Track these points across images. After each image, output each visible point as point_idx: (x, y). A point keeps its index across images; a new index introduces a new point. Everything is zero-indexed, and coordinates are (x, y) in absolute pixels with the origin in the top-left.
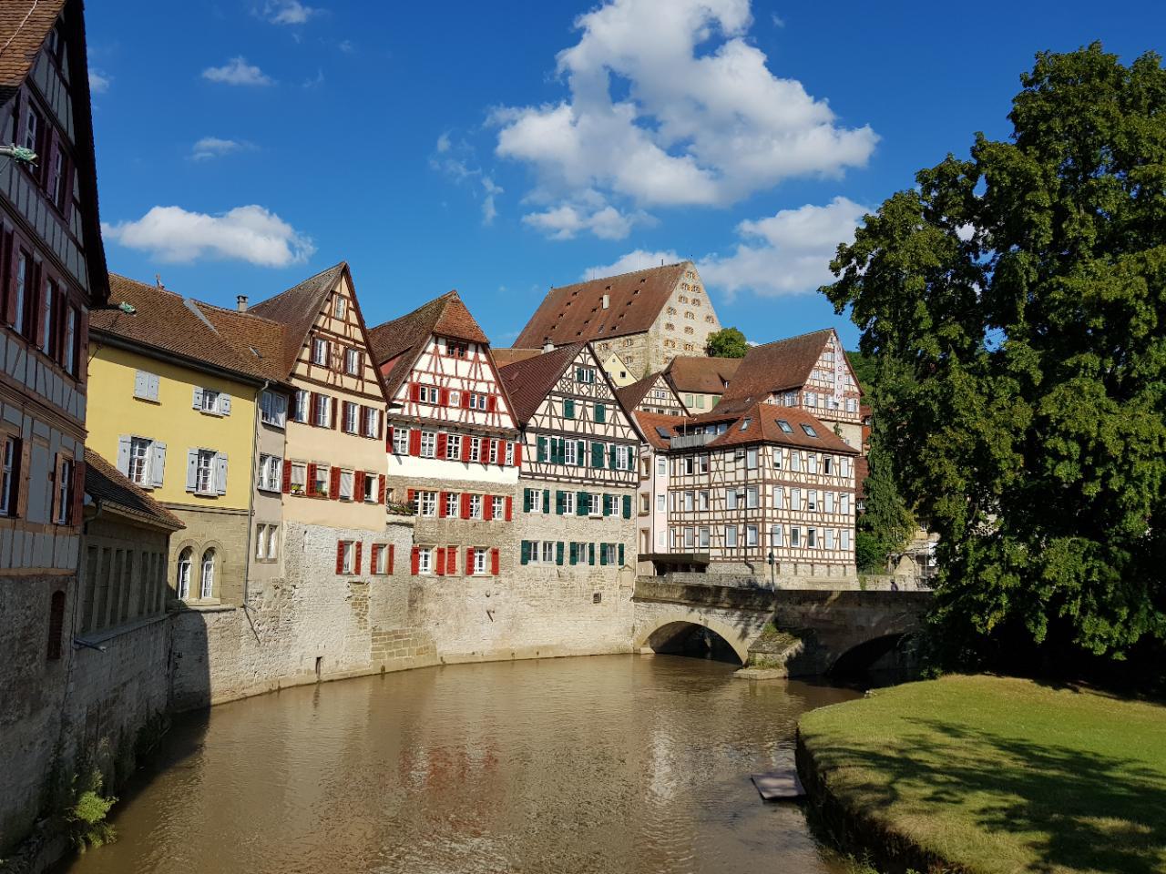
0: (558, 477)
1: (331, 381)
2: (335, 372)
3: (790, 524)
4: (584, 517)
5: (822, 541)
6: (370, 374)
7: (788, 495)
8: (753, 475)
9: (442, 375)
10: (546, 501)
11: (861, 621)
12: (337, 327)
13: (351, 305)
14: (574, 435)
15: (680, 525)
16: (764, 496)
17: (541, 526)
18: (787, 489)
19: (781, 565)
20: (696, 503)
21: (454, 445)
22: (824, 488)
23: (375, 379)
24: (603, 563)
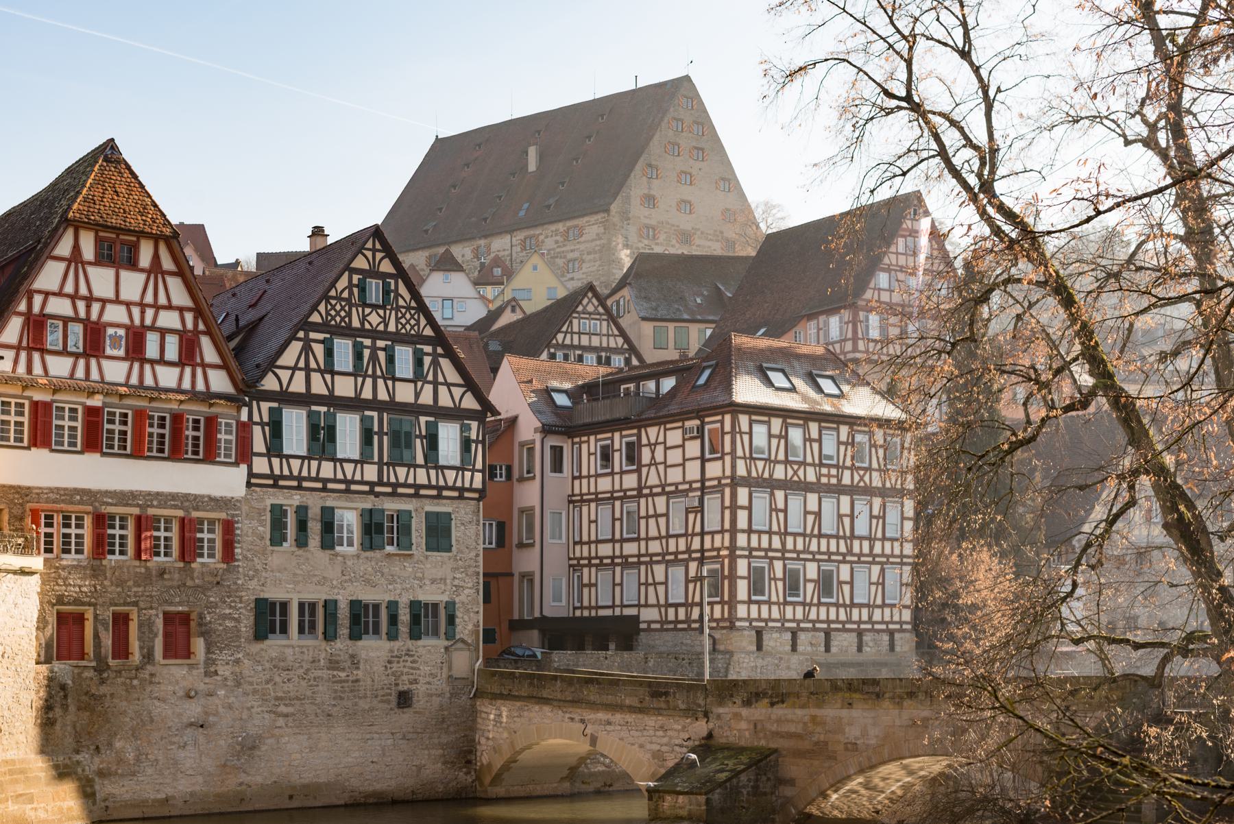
3: (783, 558)
4: (377, 554)
5: (846, 588)
7: (781, 505)
8: (714, 469)
9: (89, 300)
10: (302, 526)
11: (852, 733)
14: (354, 404)
15: (590, 565)
16: (734, 507)
18: (780, 495)
19: (765, 637)
21: (117, 427)
22: (852, 491)
24: (415, 635)
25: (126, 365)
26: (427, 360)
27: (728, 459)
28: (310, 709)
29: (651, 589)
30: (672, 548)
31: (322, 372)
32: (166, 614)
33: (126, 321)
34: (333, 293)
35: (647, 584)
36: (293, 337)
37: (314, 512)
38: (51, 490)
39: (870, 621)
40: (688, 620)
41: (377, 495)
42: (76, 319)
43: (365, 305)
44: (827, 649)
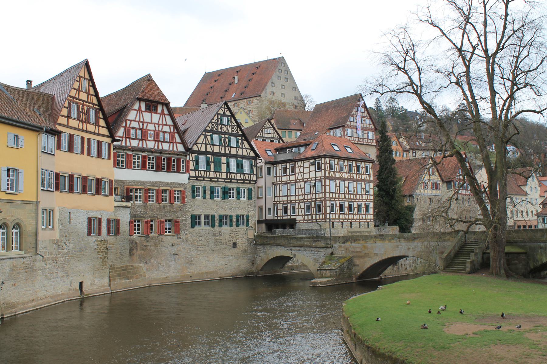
0: (211, 178)
1: (80, 127)
2: (83, 122)
3: (339, 201)
4: (226, 201)
6: (102, 123)
7: (338, 185)
9: (143, 122)
10: (205, 192)
13: (91, 84)
15: (280, 203)
16: (325, 186)
18: (338, 181)
21: (151, 162)
22: (356, 180)
23: (105, 125)
24: (237, 225)
25: (154, 142)
26: (240, 141)
27: (323, 171)
29: (300, 210)
30: (306, 198)
31: (210, 145)
33: (154, 129)
34: (213, 121)
35: (298, 209)
36: (202, 134)
37: (208, 188)
38: (132, 181)
39: (362, 219)
40: (312, 219)
41: (226, 182)
42: (139, 129)
44: (351, 227)
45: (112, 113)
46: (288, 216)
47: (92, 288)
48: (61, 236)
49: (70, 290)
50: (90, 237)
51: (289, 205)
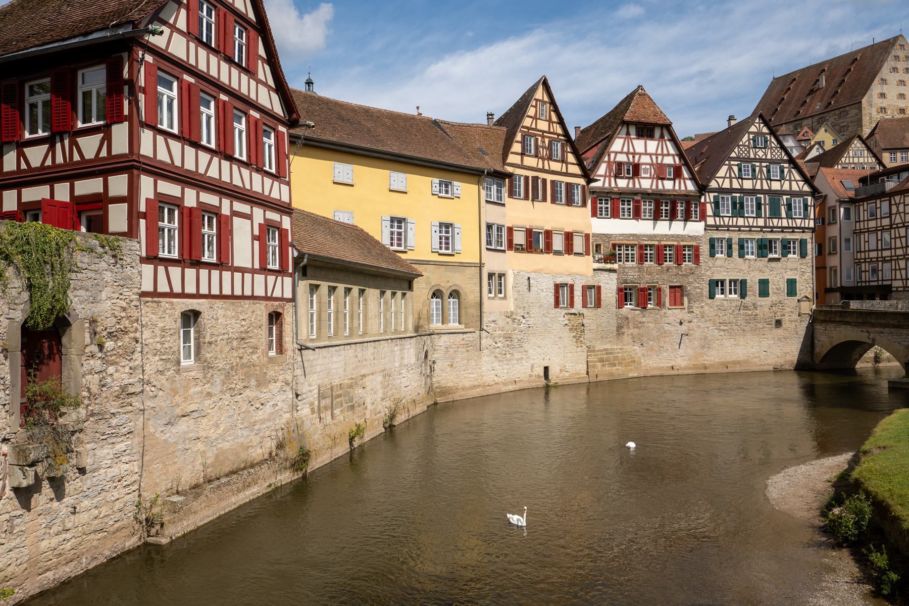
1: (540, 166)
2: (543, 159)
6: (571, 158)
9: (634, 154)
10: (730, 247)
12: (543, 125)
14: (753, 192)
17: (723, 267)
20: (879, 242)
23: (575, 162)
25: (650, 181)
26: (786, 170)
28: (735, 327)
29: (898, 272)
31: (737, 179)
32: (671, 287)
35: (896, 270)
37: (735, 241)
38: (621, 235)
41: (764, 232)
43: (755, 148)
45: (588, 145)
46: (878, 281)
47: (561, 375)
48: (518, 307)
49: (530, 376)
50: (558, 310)
51: (880, 263)
